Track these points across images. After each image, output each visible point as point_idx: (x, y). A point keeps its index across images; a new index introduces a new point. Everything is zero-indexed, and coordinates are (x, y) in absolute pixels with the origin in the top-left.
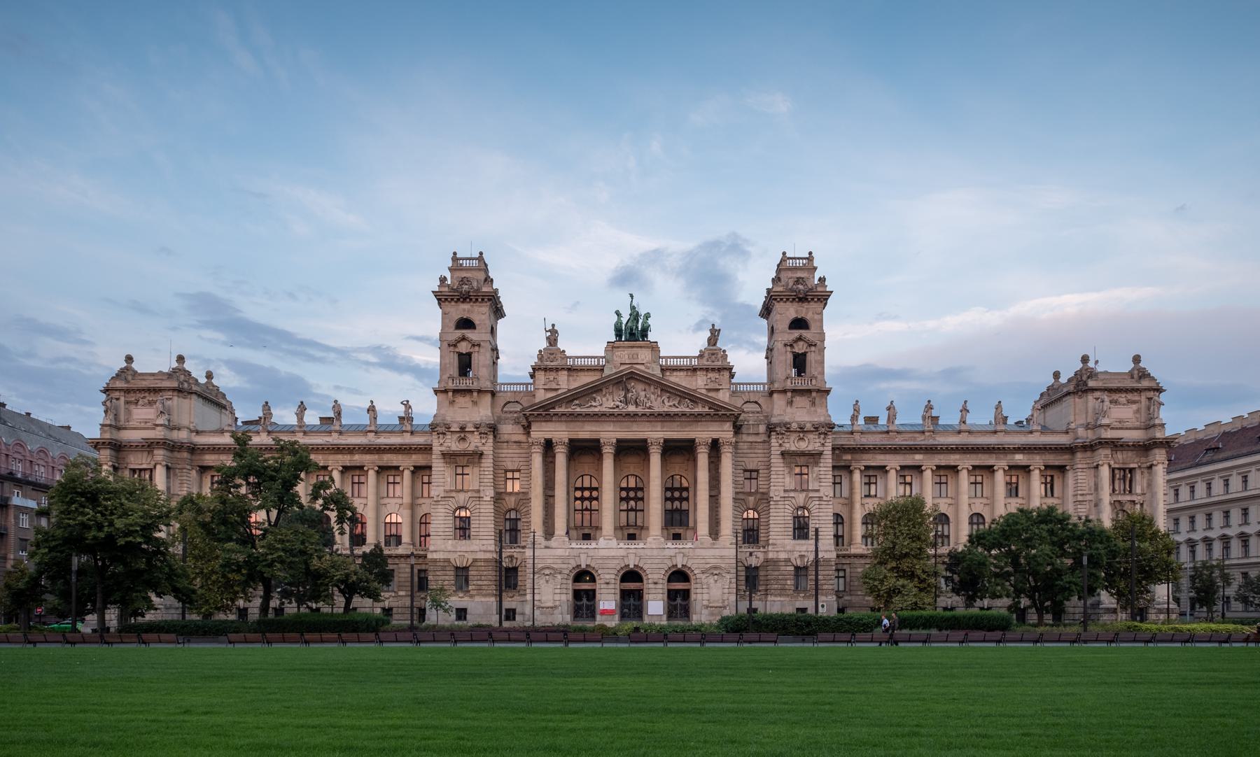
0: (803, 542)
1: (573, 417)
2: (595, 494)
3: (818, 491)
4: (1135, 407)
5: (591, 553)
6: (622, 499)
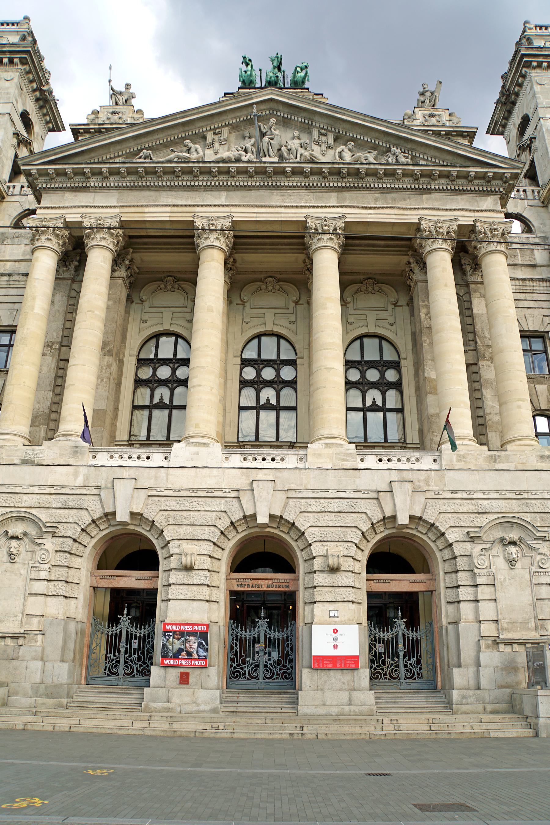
5: (147, 480)
6: (244, 383)
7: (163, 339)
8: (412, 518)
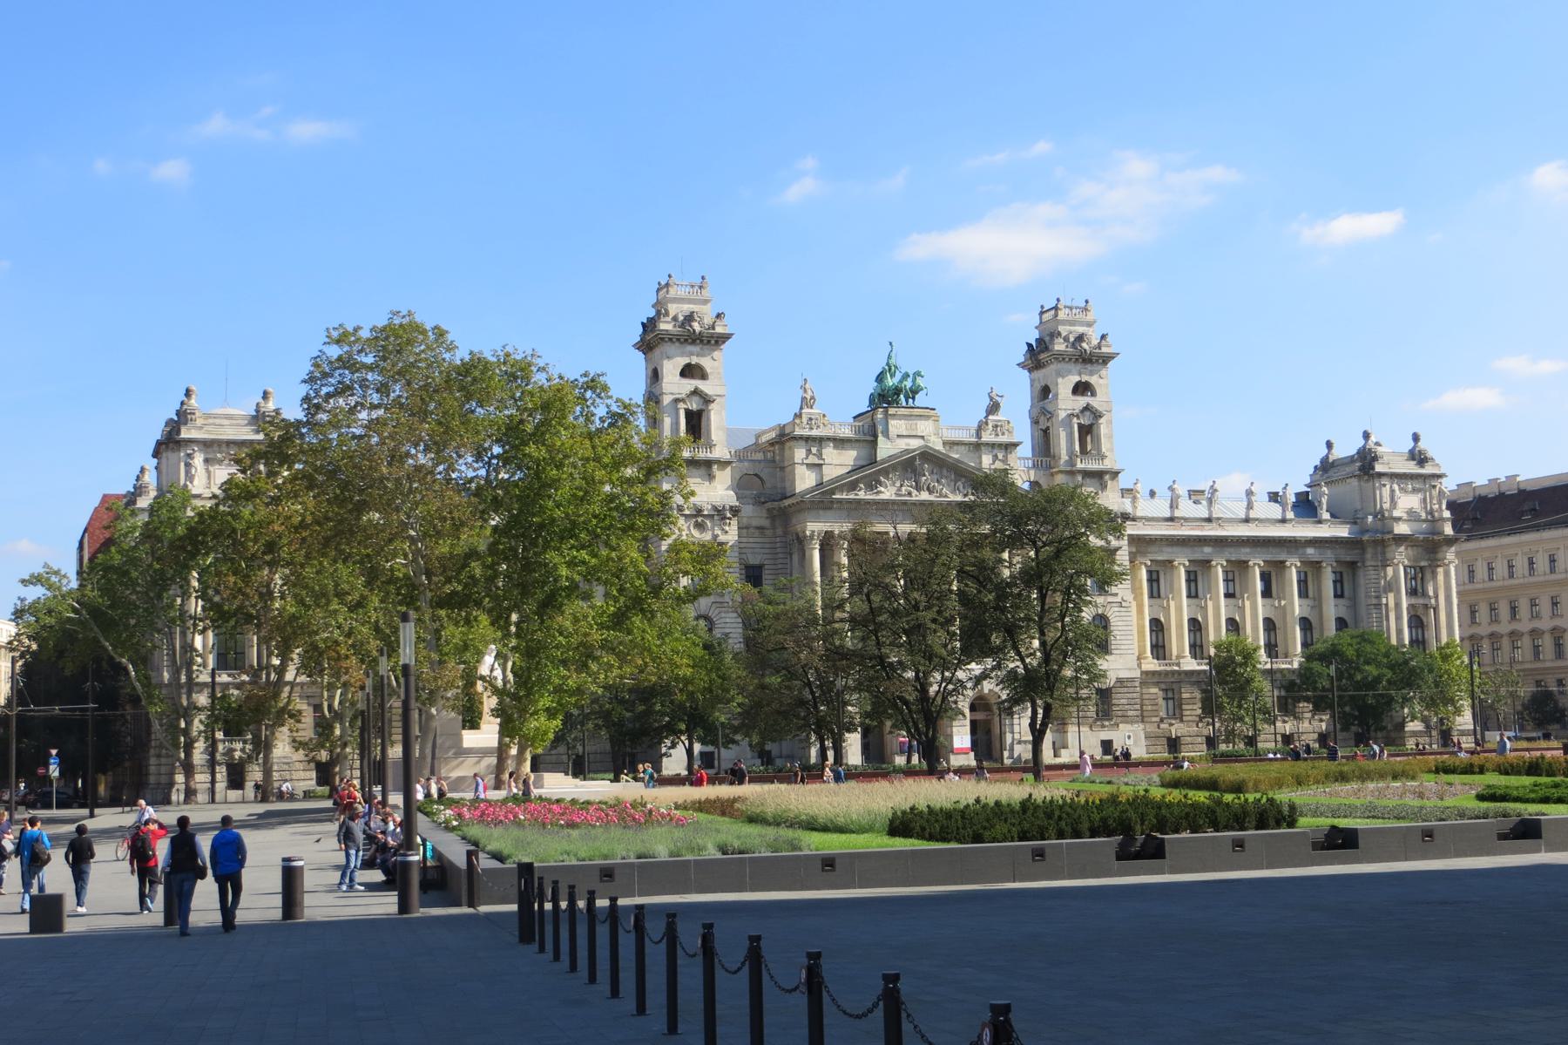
4: (1420, 496)
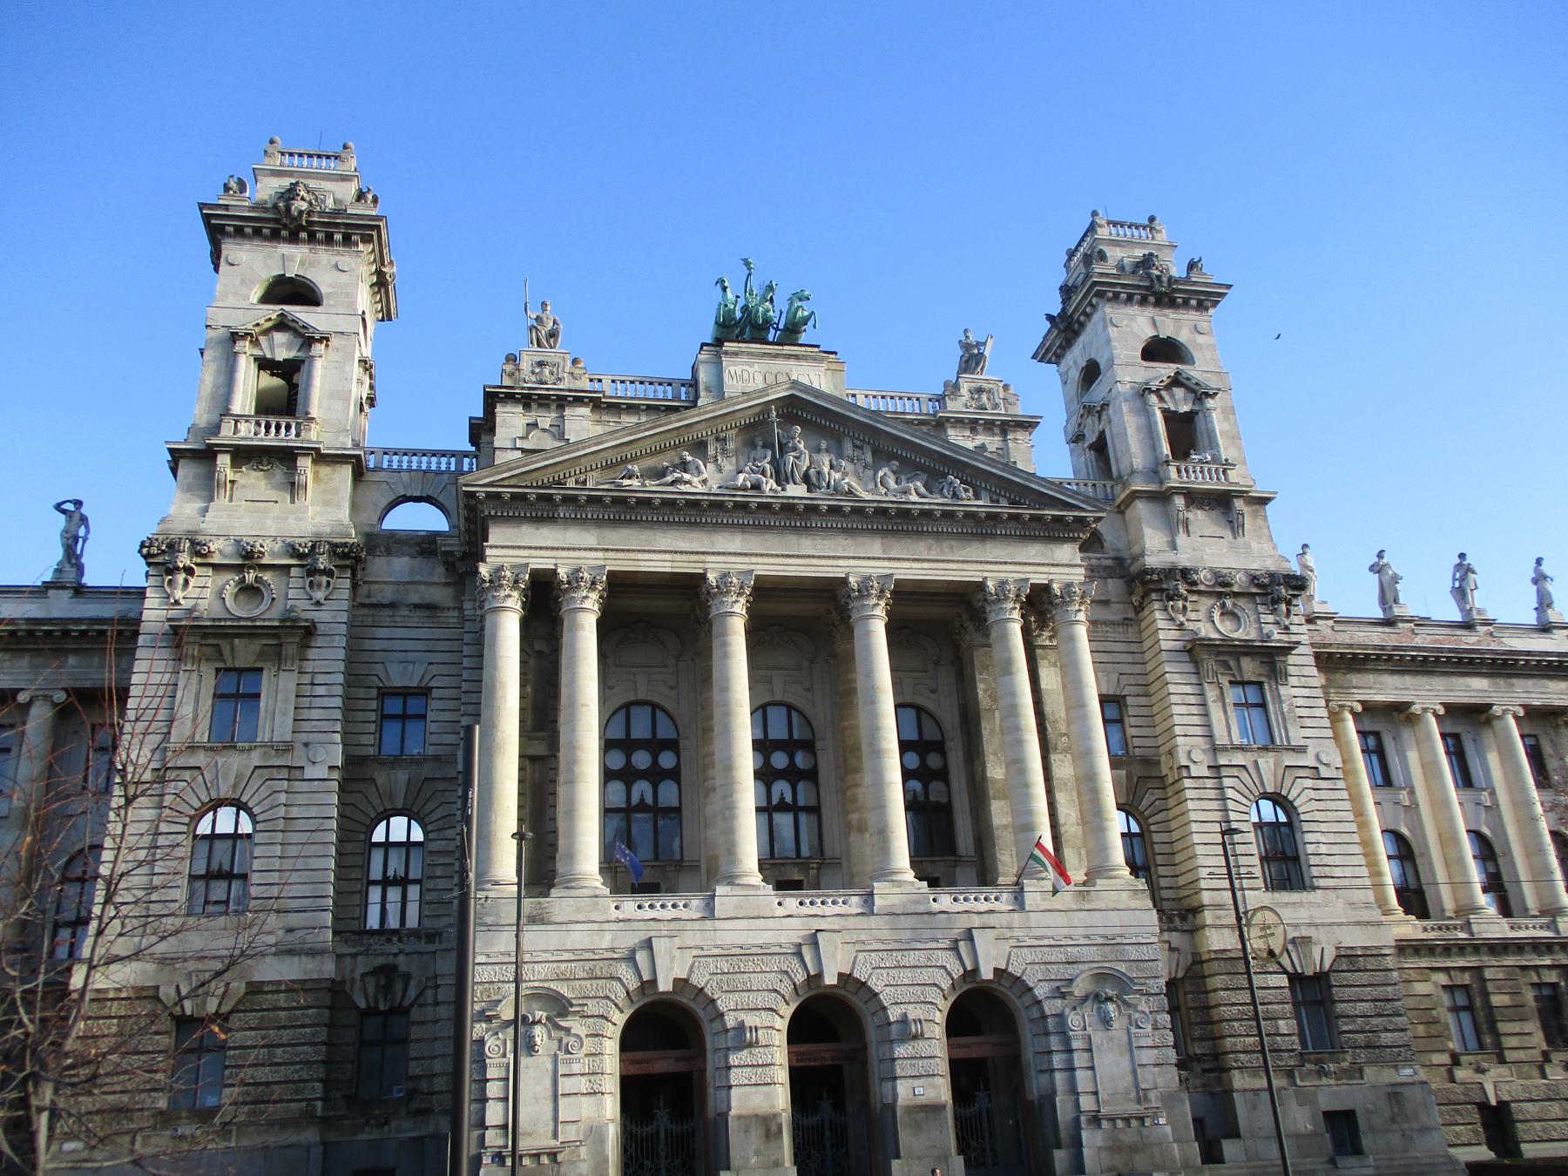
0: (1294, 896)
1: (623, 511)
2: (667, 760)
3: (1301, 750)
7: (634, 710)
8: (996, 970)
